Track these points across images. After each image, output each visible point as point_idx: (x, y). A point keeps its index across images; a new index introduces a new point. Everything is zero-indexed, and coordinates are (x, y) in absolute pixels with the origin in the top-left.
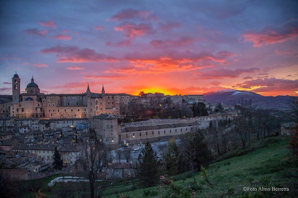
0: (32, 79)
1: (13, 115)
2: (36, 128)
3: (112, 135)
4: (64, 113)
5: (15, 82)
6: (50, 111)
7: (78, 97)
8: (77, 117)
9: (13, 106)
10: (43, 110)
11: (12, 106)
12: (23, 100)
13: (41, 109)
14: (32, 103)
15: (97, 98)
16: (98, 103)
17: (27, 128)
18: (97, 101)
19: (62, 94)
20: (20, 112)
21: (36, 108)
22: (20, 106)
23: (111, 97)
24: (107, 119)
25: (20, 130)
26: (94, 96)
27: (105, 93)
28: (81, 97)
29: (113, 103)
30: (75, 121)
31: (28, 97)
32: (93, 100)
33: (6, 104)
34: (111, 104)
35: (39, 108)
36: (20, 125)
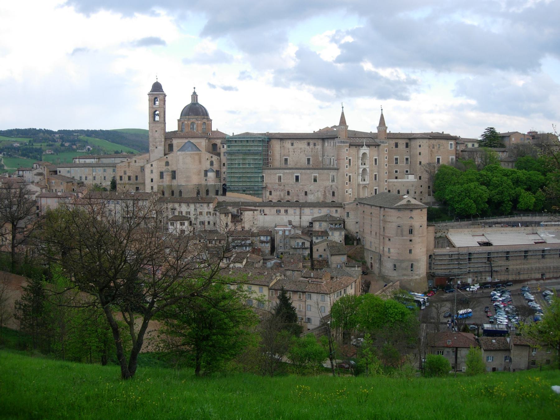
0: (195, 93)
1: (152, 188)
2: (209, 223)
3: (410, 251)
4: (276, 186)
5: (155, 104)
7: (312, 142)
8: (311, 198)
9: (152, 165)
10: (223, 176)
11: (149, 165)
12: (175, 148)
13: (218, 173)
14: (197, 157)
15: (368, 146)
16: (367, 162)
17: (187, 223)
18: (364, 154)
19: (268, 133)
20: (167, 178)
21: (206, 172)
22: (167, 164)
23: (402, 143)
24: (399, 209)
25: (170, 227)
26: (357, 140)
27: (388, 132)
28: (320, 142)
30: (307, 211)
31: (186, 141)
32: (353, 150)
33: (134, 159)
34: (402, 164)
35: (214, 171)
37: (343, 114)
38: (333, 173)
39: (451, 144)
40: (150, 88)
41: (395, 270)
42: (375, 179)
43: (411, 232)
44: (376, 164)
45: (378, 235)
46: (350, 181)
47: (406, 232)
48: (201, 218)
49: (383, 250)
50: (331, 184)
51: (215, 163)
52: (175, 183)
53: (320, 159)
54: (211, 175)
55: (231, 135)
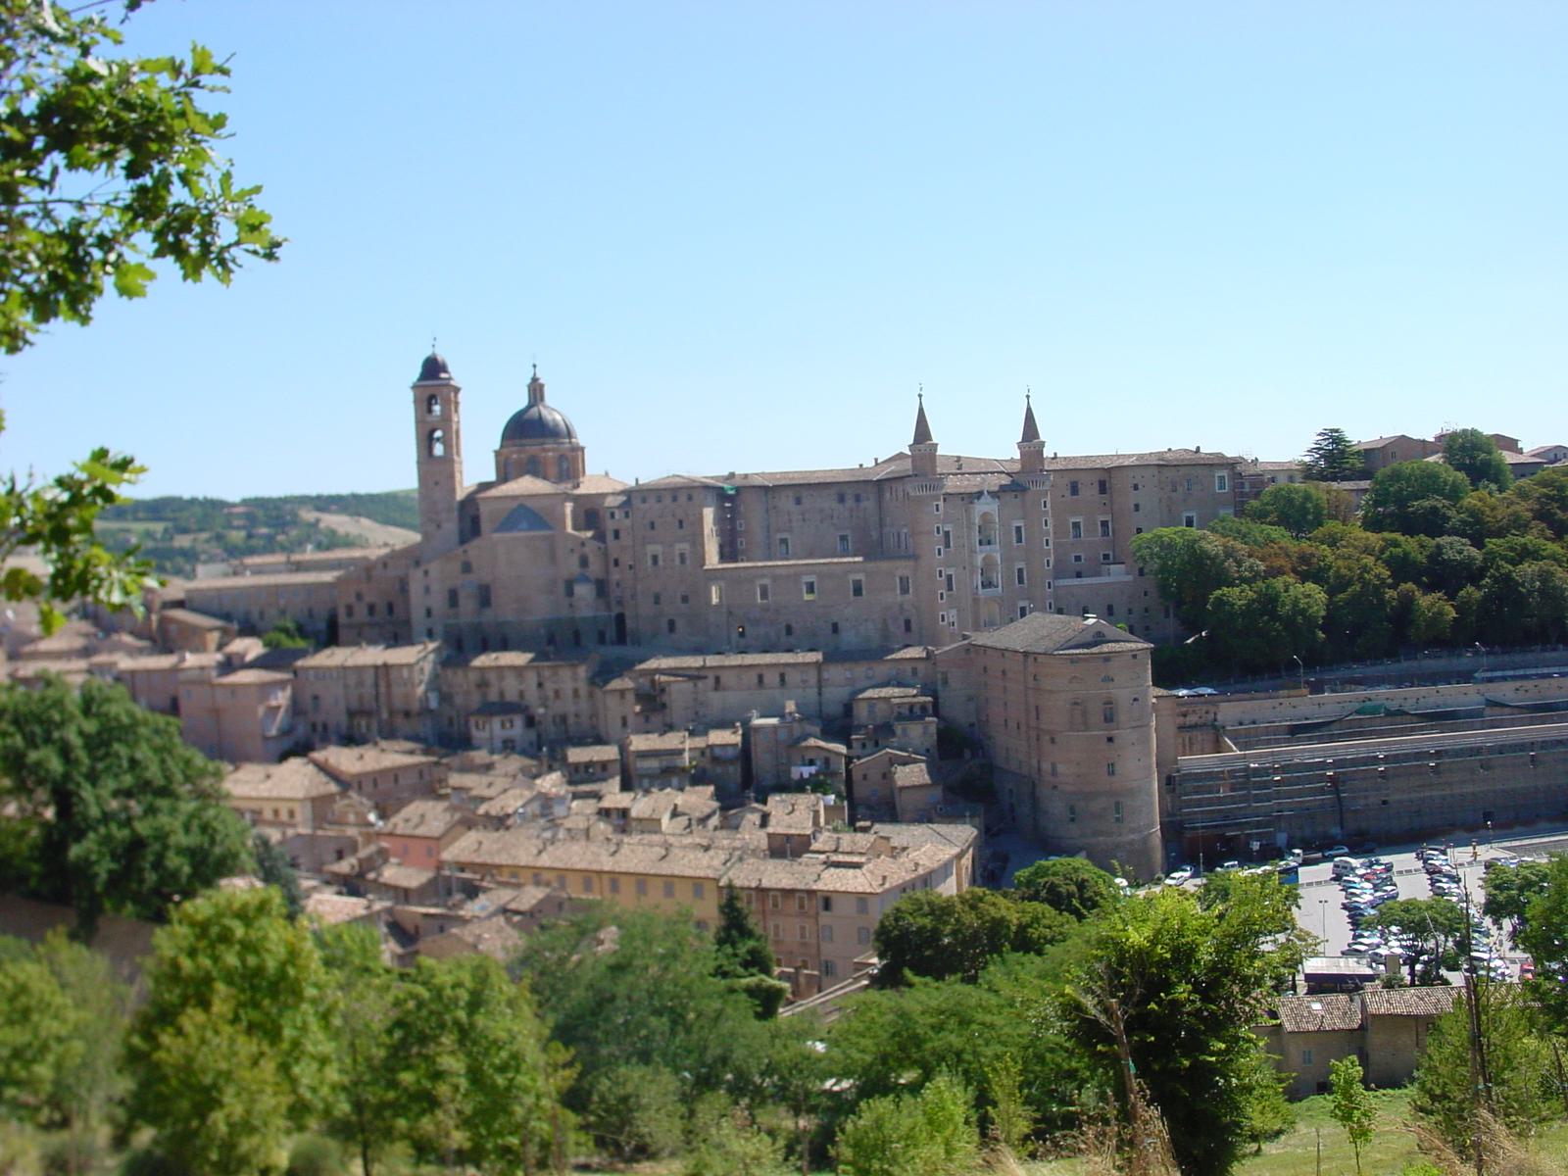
0: (535, 380)
3: (1112, 773)
5: (430, 411)
6: (657, 600)
9: (426, 573)
10: (615, 593)
12: (485, 526)
13: (602, 588)
17: (519, 720)
18: (985, 515)
20: (468, 604)
22: (467, 568)
29: (1105, 533)
36: (475, 700)
37: (921, 411)
38: (903, 568)
39: (1222, 478)
40: (416, 372)
41: (1073, 820)
42: (1021, 581)
43: (1109, 718)
44: (1019, 540)
45: (1023, 728)
46: (950, 588)
47: (1096, 717)
48: (558, 708)
49: (1039, 769)
50: (899, 598)
51: (591, 559)
52: (489, 616)
53: (875, 535)
54: (584, 591)
55: (633, 484)
